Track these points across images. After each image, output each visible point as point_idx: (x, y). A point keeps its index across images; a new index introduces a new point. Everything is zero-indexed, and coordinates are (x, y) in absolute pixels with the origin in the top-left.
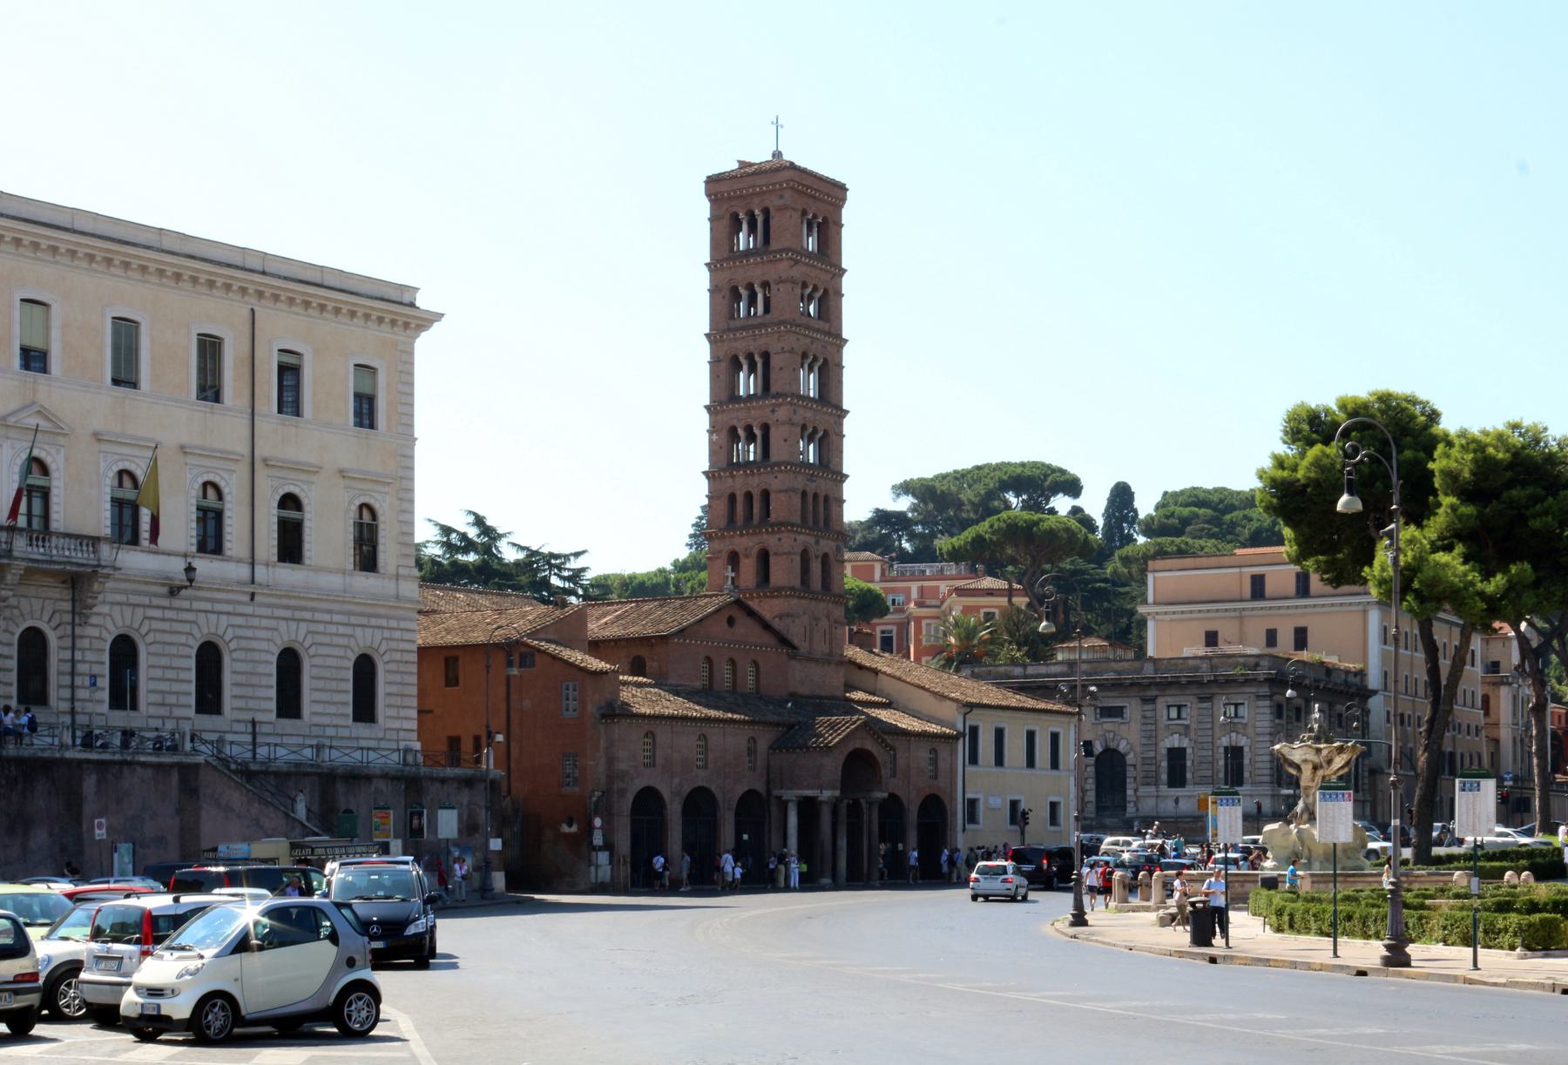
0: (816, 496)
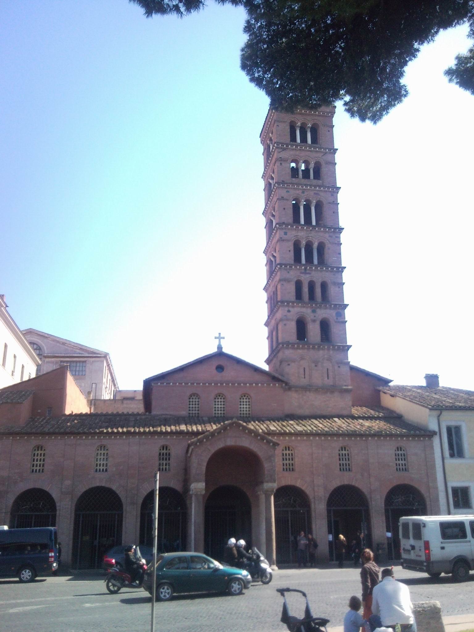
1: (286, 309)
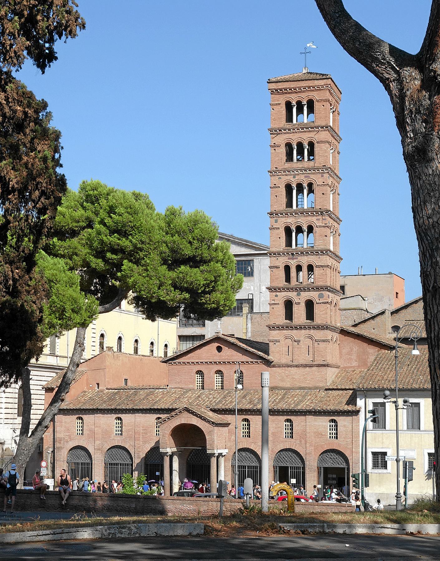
1: (274, 294)
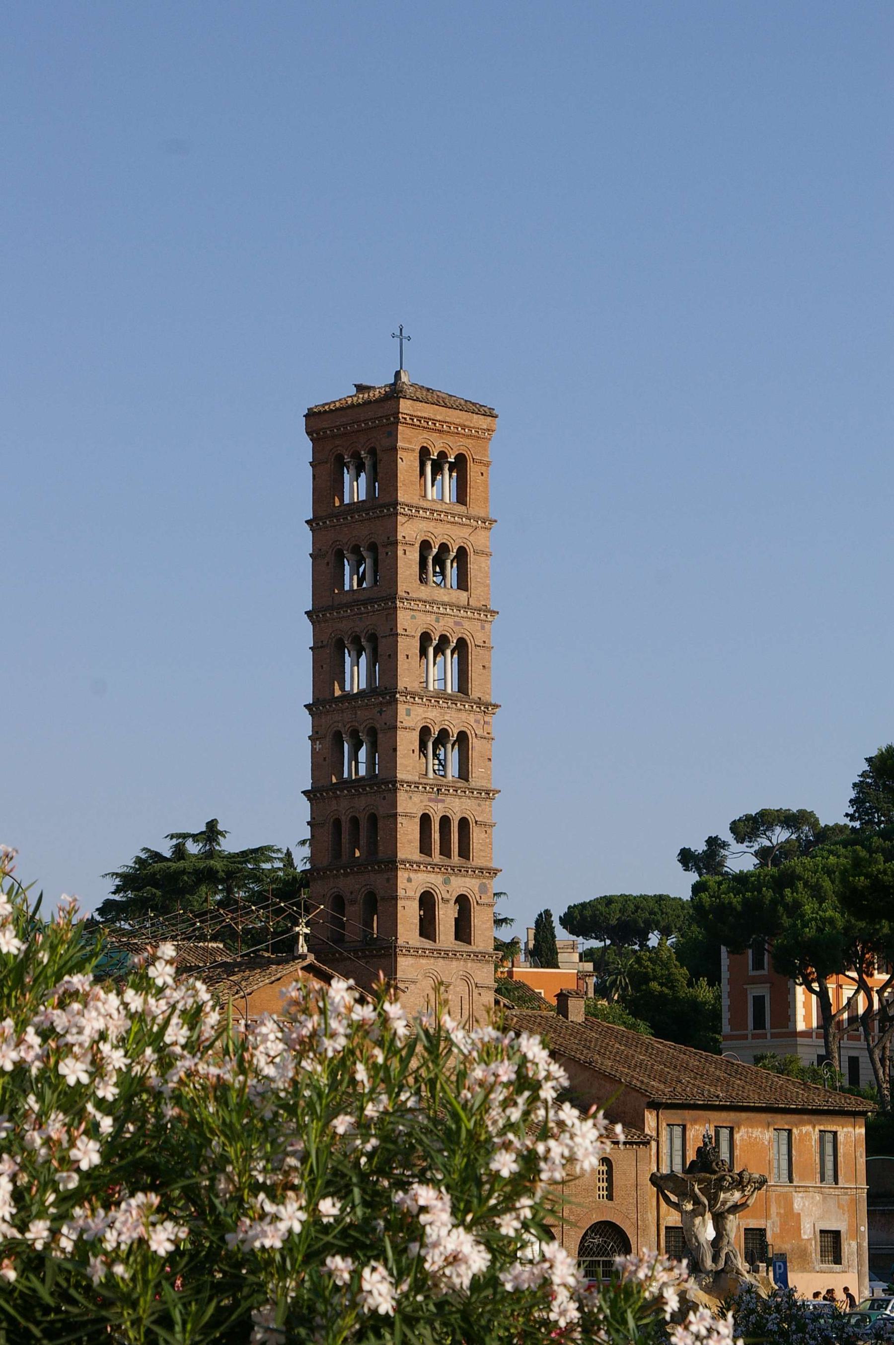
0: (445, 821)
1: (406, 875)
